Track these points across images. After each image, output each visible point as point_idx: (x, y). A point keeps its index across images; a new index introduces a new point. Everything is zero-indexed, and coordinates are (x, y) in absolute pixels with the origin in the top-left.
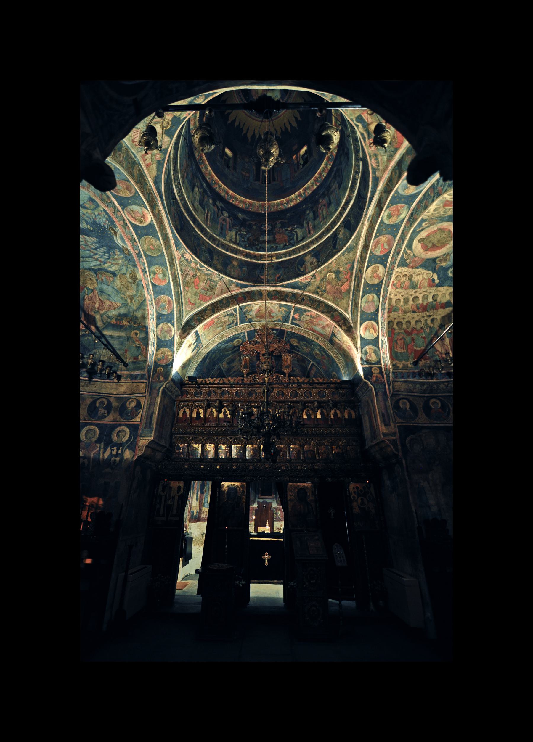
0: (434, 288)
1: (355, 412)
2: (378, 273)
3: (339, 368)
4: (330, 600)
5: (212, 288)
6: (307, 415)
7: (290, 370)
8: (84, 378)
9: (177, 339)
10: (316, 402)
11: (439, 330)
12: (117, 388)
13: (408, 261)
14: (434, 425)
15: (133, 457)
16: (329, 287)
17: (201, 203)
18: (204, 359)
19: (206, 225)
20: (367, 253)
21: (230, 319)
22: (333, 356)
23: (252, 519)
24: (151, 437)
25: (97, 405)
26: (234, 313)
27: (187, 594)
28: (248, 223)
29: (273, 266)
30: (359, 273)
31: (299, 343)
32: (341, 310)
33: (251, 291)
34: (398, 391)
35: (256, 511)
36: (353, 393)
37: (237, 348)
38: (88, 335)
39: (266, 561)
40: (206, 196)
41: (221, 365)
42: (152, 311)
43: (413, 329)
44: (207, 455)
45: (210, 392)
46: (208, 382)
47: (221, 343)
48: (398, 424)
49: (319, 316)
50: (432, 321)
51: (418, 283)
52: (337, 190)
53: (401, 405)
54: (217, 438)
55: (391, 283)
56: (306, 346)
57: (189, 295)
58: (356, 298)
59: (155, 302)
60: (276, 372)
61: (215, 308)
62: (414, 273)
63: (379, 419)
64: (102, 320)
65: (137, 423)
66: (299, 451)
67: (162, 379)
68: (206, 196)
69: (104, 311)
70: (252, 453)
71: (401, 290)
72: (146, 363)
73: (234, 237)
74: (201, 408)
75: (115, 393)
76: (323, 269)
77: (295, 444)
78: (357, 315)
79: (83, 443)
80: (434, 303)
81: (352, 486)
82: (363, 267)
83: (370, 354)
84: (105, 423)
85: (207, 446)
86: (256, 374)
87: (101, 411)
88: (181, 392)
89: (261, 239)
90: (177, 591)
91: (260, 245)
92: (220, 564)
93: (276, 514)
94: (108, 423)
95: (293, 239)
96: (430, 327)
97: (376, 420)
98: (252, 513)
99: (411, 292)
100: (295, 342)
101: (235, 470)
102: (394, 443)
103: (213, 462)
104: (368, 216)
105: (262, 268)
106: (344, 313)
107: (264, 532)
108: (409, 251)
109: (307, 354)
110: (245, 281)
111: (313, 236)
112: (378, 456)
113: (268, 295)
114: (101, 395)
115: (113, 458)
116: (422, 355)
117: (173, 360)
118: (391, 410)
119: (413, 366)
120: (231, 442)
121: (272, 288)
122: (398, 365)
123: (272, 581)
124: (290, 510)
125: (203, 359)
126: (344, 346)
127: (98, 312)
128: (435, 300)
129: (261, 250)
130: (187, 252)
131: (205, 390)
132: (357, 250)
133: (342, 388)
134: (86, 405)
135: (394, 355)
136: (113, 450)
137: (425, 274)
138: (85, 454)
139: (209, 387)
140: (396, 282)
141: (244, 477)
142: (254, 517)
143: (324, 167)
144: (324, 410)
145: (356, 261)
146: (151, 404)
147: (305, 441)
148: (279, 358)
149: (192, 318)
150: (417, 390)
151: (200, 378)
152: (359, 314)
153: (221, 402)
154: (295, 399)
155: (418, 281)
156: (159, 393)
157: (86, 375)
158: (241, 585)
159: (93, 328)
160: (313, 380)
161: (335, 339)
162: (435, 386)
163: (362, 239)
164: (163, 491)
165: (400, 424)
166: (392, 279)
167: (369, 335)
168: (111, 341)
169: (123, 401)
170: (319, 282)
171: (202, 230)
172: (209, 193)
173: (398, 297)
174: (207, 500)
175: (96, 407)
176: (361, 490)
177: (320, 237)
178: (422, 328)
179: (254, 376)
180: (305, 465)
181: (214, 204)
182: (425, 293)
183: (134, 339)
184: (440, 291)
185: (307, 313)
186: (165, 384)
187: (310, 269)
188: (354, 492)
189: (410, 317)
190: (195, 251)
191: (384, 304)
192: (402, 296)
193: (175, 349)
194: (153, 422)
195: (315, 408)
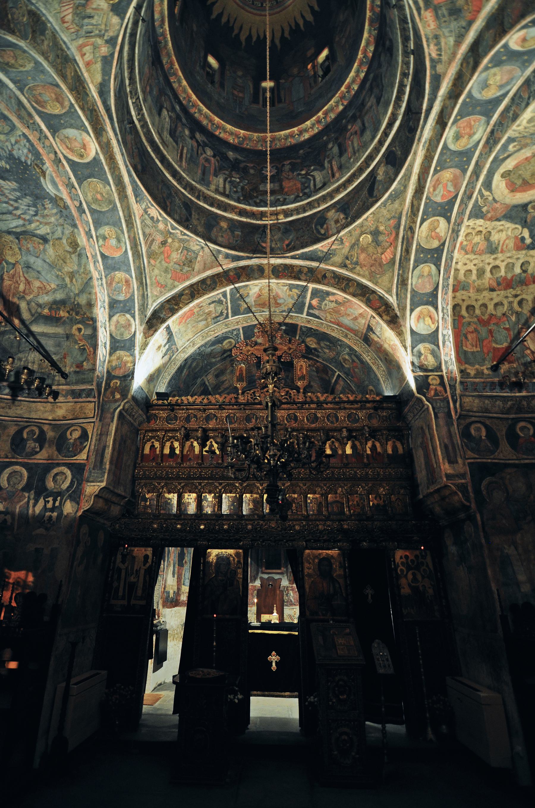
0: (524, 252)
1: (403, 444)
2: (438, 230)
3: (379, 380)
4: (367, 723)
5: (191, 261)
6: (331, 449)
7: (306, 382)
8: (5, 397)
9: (139, 338)
10: (344, 430)
11: (530, 318)
12: (52, 411)
13: (484, 209)
14: (522, 462)
15: (77, 511)
16: (362, 256)
17: (173, 133)
18: (180, 369)
19: (180, 166)
20: (421, 200)
21: (218, 308)
22: (369, 361)
23: (253, 604)
24: (102, 482)
25: (25, 436)
26: (222, 298)
27: (159, 712)
28: (242, 165)
29: (279, 229)
30: (409, 233)
31: (319, 344)
32: (381, 291)
33: (248, 266)
34: (469, 411)
35: (258, 591)
36: (400, 415)
37: (229, 353)
38: (9, 332)
39: (274, 664)
40: (179, 124)
41: (206, 379)
42: (101, 297)
43: (491, 315)
44: (186, 510)
45: (189, 416)
46: (186, 402)
47: (204, 345)
48: (469, 461)
49: (349, 301)
50: (520, 303)
51: (499, 244)
52: (374, 107)
53: (473, 432)
54: (200, 484)
55: (458, 245)
56: (330, 348)
57: (156, 271)
58: (403, 271)
59: (106, 283)
60: (286, 385)
61: (195, 291)
62: (493, 229)
63: (440, 453)
64: (29, 310)
65: (82, 462)
66: (321, 503)
67: (118, 396)
68: (179, 124)
69: (32, 296)
70: (251, 506)
71: (472, 256)
72: (94, 373)
73: (221, 186)
74: (176, 440)
75: (50, 418)
76: (354, 229)
77: (314, 493)
78: (406, 298)
79: (5, 492)
80: (524, 275)
81: (399, 554)
82: (415, 222)
83: (426, 356)
84: (36, 461)
85: (186, 495)
86: (256, 390)
87: (31, 444)
88: (147, 416)
89: (261, 188)
90: (145, 708)
91: (260, 197)
92: (206, 670)
93: (287, 595)
94: (41, 461)
95: (309, 187)
96: (517, 313)
97: (436, 455)
98: (252, 594)
99: (489, 259)
100: (312, 343)
101: (226, 531)
102: (463, 488)
103: (195, 520)
104: (423, 140)
105: (264, 232)
106: (386, 295)
107: (269, 622)
108: (486, 193)
109: (331, 360)
110: (238, 251)
111: (338, 180)
112: (437, 509)
113: (272, 271)
114: (30, 421)
115: (48, 514)
116: (505, 356)
117: (134, 369)
118: (458, 440)
119: (491, 373)
120: (220, 490)
121: (279, 261)
122: (468, 371)
123: (283, 694)
124: (307, 590)
125: (179, 369)
126: (386, 346)
127: (23, 297)
128: (525, 271)
129: (262, 204)
130: (152, 205)
131: (181, 414)
132: (406, 197)
133: (383, 409)
134: (8, 436)
135: (462, 356)
136: (48, 502)
137: (510, 230)
138: (7, 508)
139: (187, 409)
140: (465, 243)
141: (241, 541)
142: (256, 601)
143: (355, 75)
144: (357, 443)
145: (404, 213)
146: (103, 434)
147: (328, 487)
148: (289, 366)
149: (162, 306)
150: (497, 408)
151: (174, 396)
152: (409, 296)
153: (205, 431)
154: (313, 425)
155: (499, 241)
157: (7, 391)
158: (236, 701)
159: (16, 322)
160: (340, 398)
161: (373, 336)
162: (525, 403)
163: (414, 178)
164: (123, 562)
165: (472, 461)
166: (460, 239)
167: (424, 328)
168: (43, 341)
169: (61, 430)
170: (347, 249)
171: (175, 174)
172: (184, 120)
173: (468, 267)
174: (187, 574)
175: (23, 439)
176: (412, 561)
177: (350, 181)
178: (504, 314)
179: (254, 393)
180: (329, 523)
181: (192, 137)
182: (510, 260)
183: (77, 338)
184: (532, 256)
185: (331, 298)
187: (335, 231)
188: (402, 563)
189: (486, 299)
190: (163, 205)
191: (446, 279)
192: (475, 265)
193: (137, 352)
194: (105, 460)
195: (343, 438)
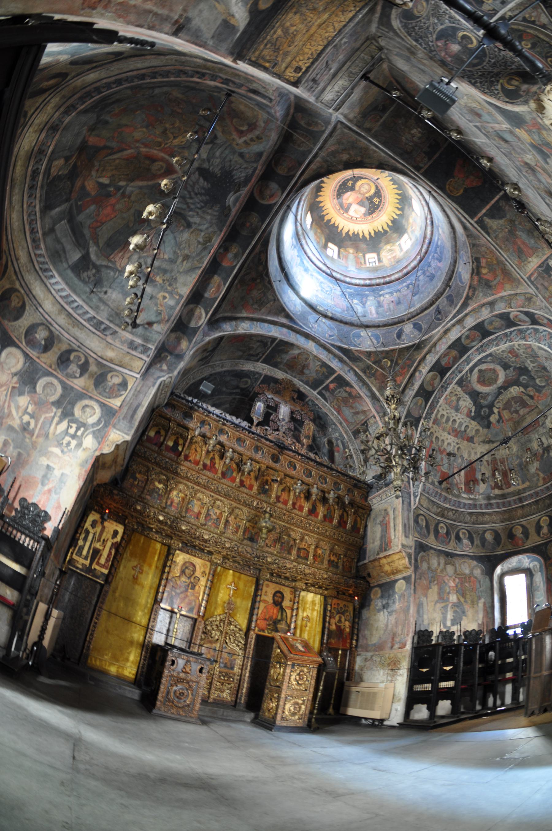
43: (445, 449)
50: (459, 448)
99: (454, 413)
118: (412, 523)
128: (465, 431)
166: (447, 393)
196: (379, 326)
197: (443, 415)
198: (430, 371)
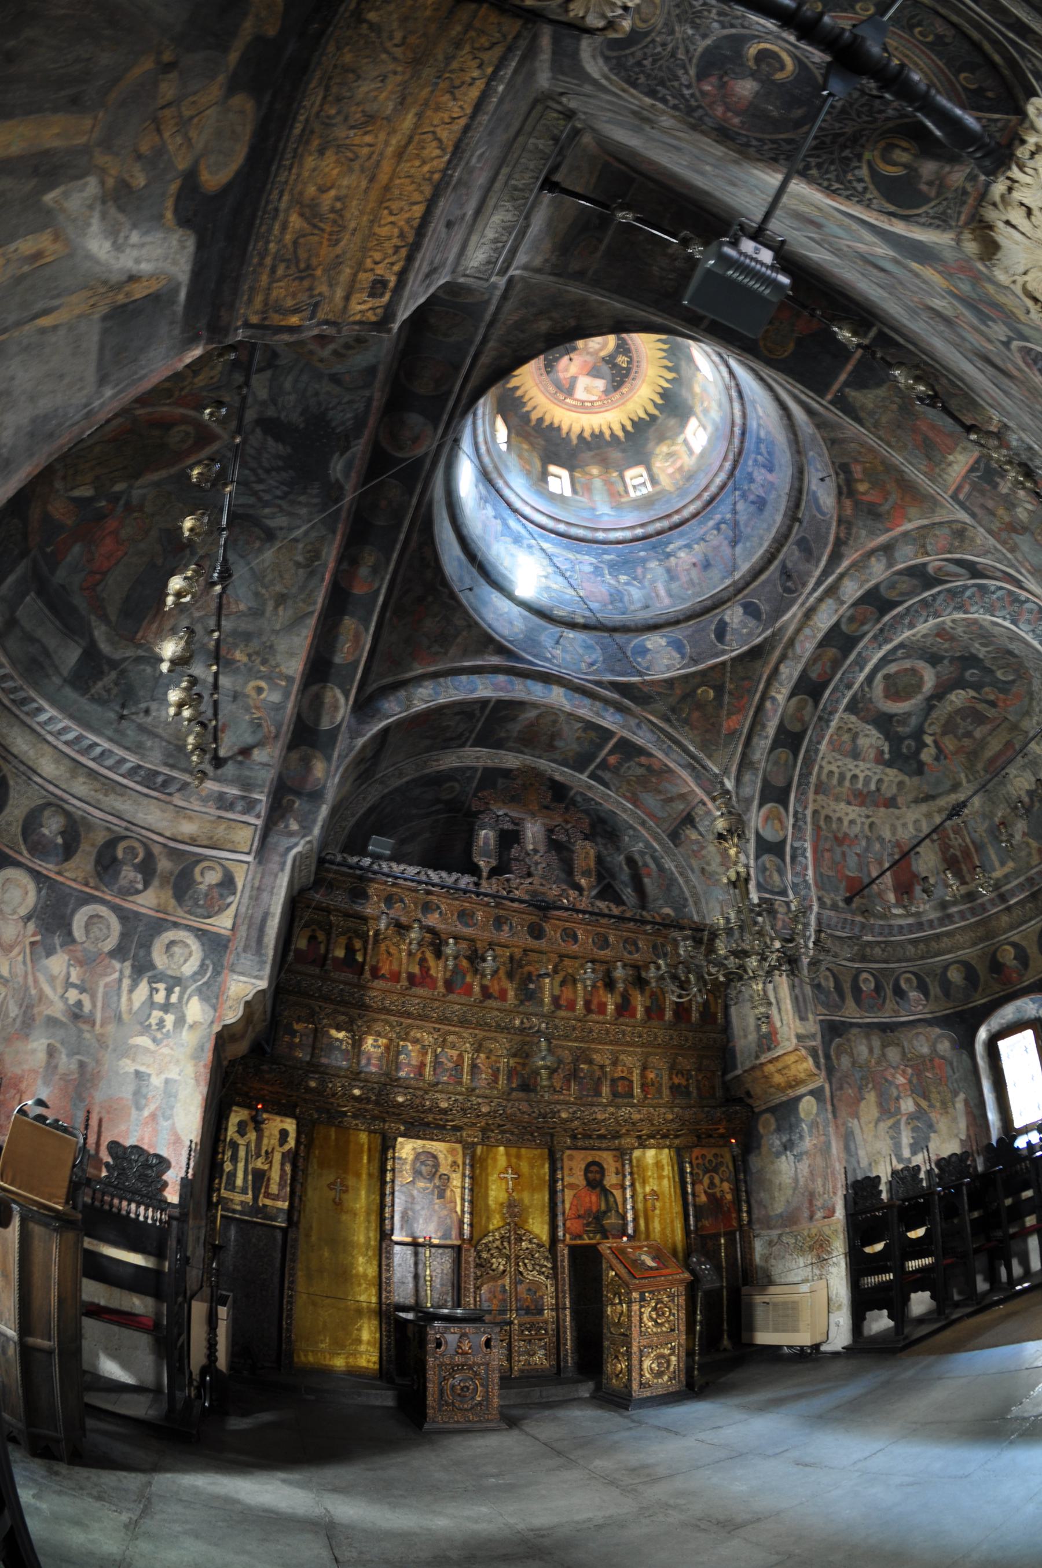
43: (846, 835)
50: (872, 825)
99: (851, 764)
128: (878, 790)
156: (284, 864)
166: (831, 731)
186: (302, 842)
196: (677, 622)
197: (831, 772)
198: (792, 695)
